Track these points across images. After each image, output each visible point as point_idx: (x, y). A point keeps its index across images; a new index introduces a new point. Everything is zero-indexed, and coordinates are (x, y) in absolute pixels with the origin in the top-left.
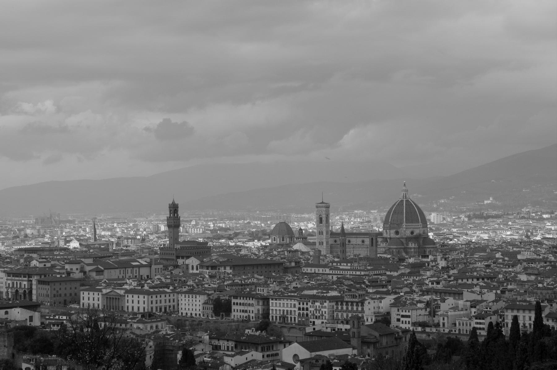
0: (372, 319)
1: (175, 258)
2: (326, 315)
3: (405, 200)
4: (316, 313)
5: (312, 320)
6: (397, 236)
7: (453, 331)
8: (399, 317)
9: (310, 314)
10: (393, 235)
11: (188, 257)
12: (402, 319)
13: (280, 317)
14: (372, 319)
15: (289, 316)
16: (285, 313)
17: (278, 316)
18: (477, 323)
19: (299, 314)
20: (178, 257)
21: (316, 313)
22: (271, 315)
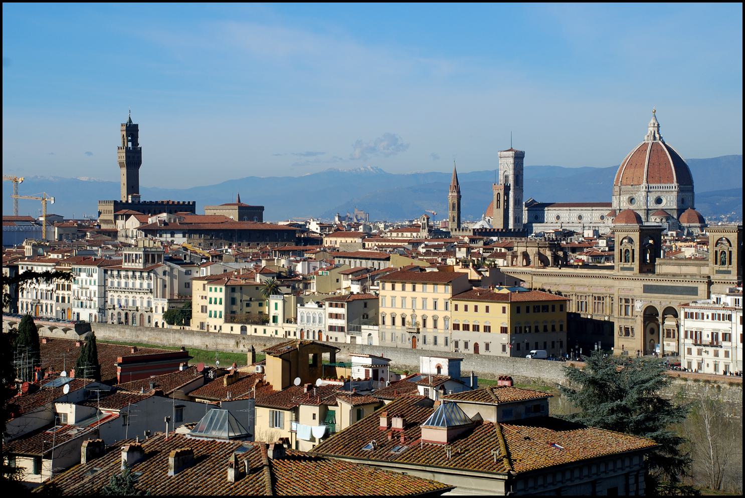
0: (163, 308)
1: (112, 218)
2: (96, 299)
3: (650, 142)
4: (82, 295)
5: (76, 310)
6: (632, 207)
7: (292, 334)
8: (205, 302)
9: (72, 298)
10: (625, 205)
11: (128, 217)
12: (211, 307)
13: (32, 305)
14: (163, 308)
15: (44, 302)
16: (39, 297)
17: (30, 301)
18: (331, 316)
19: (58, 298)
20: (116, 217)
21: (82, 295)
22: (20, 300)
